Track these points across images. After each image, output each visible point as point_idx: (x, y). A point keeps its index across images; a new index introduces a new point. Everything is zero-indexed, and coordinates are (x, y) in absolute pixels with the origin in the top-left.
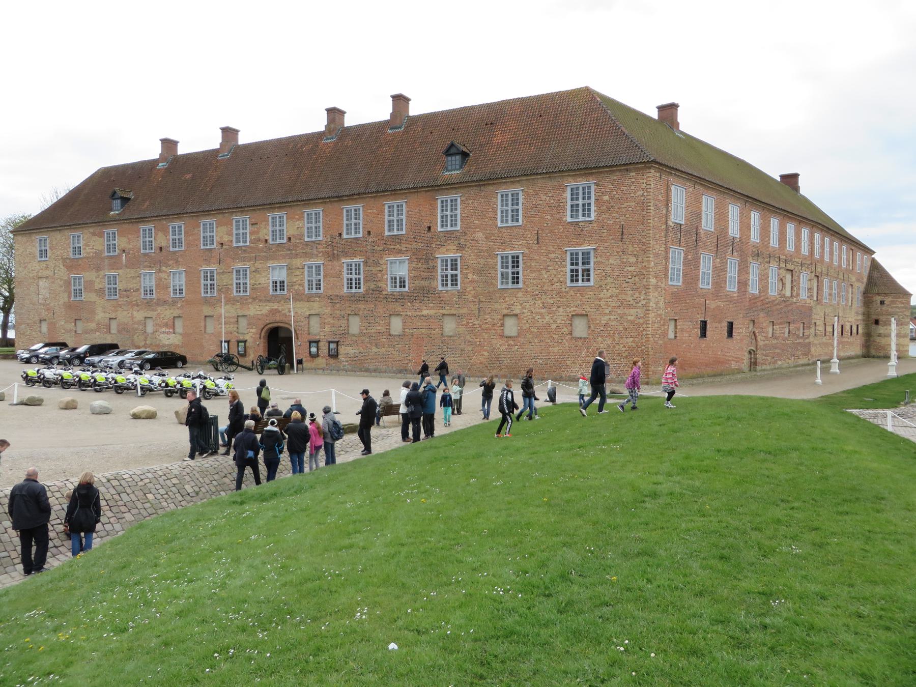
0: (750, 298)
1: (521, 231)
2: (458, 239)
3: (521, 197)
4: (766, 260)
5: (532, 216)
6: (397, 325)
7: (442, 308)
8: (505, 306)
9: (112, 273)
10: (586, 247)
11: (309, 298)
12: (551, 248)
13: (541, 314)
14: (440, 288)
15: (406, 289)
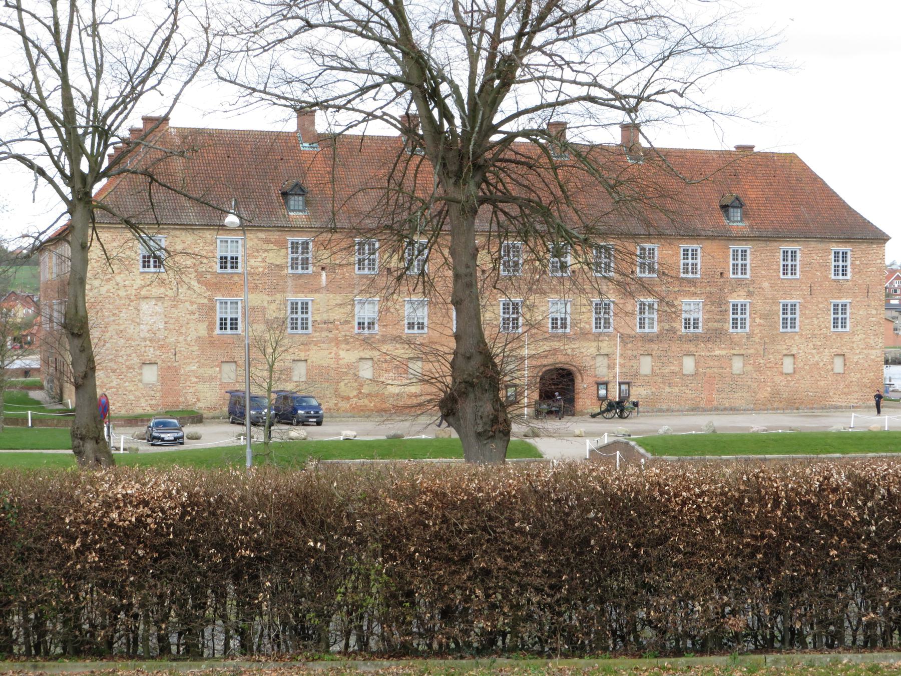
1: (798, 284)
2: (747, 286)
3: (798, 255)
5: (807, 272)
6: (689, 365)
7: (733, 349)
8: (785, 347)
9: (300, 298)
10: (844, 301)
11: (598, 337)
12: (820, 299)
13: (812, 354)
14: (731, 330)
15: (700, 330)
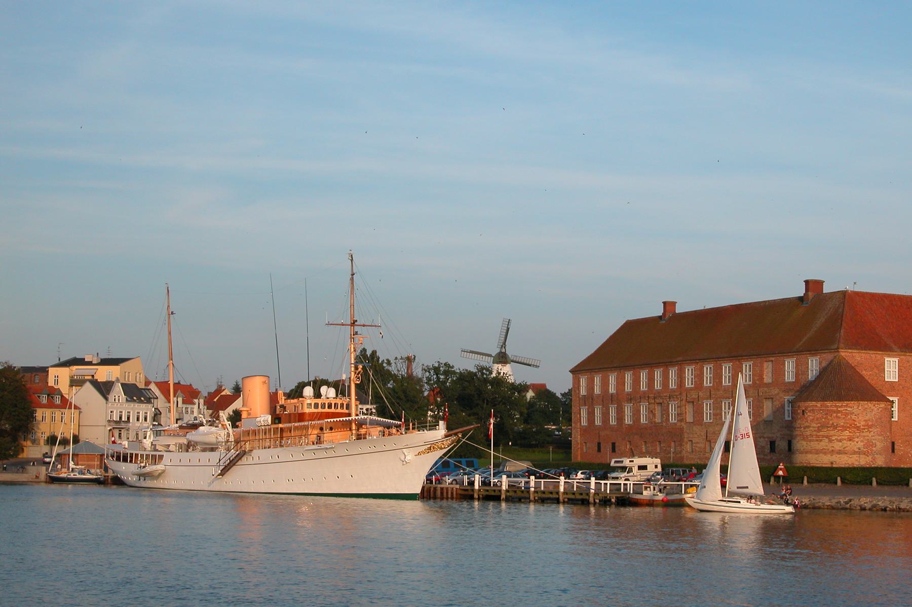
0: (626, 428)
4: (638, 400)
